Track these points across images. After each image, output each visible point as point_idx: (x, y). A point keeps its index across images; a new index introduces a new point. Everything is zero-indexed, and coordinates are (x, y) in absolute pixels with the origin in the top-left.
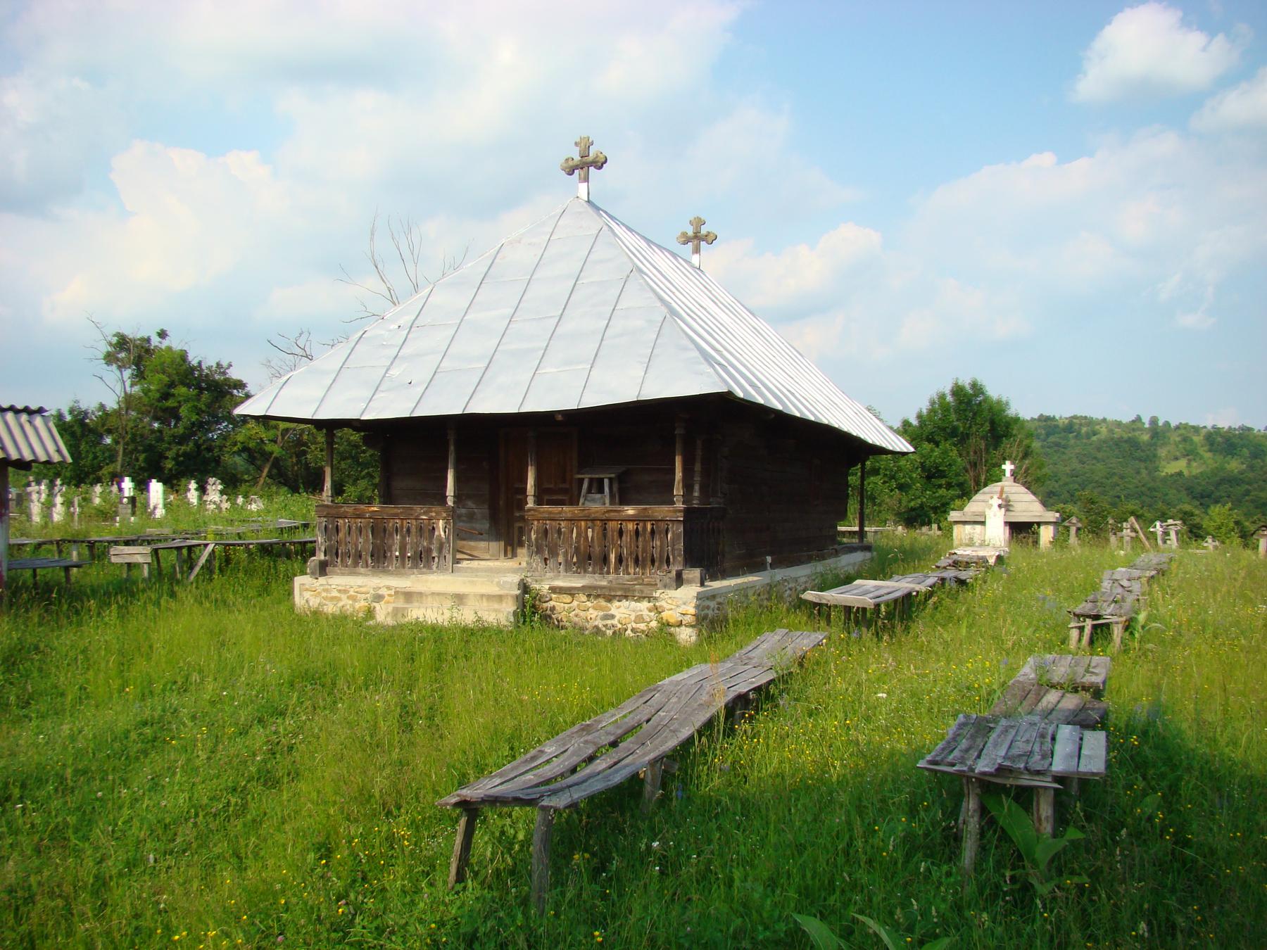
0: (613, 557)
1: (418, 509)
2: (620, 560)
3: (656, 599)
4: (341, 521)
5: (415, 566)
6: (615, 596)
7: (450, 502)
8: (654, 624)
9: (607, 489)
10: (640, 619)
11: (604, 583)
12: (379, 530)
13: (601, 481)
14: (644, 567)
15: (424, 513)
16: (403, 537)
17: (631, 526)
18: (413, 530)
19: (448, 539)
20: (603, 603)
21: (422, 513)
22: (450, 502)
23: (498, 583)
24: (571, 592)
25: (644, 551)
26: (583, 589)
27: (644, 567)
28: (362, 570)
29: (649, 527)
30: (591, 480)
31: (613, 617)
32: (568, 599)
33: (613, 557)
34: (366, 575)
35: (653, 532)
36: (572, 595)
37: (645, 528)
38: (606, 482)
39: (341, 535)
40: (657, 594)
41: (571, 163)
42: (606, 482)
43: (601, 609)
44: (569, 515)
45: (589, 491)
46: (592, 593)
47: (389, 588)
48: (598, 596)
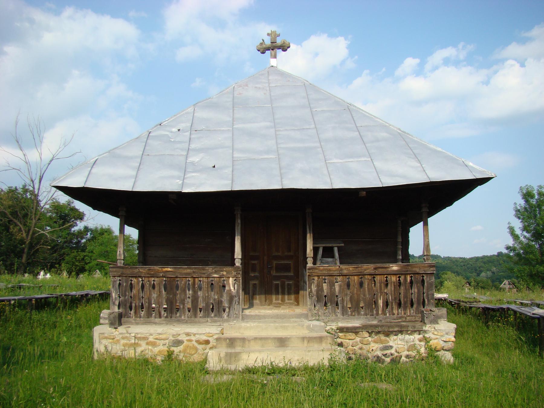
0: (381, 302)
1: (210, 269)
2: (386, 304)
3: (425, 332)
4: (134, 280)
5: (207, 316)
6: (392, 332)
7: (238, 263)
8: (423, 350)
9: (337, 255)
10: (412, 347)
11: (375, 322)
12: (171, 286)
13: (331, 249)
14: (405, 309)
15: (216, 272)
16: (195, 292)
17: (394, 279)
18: (204, 286)
19: (238, 292)
20: (383, 337)
21: (214, 273)
22: (238, 263)
23: (308, 327)
24: (355, 331)
25: (406, 296)
26: (364, 327)
27: (405, 309)
28: (158, 320)
29: (409, 279)
30: (324, 248)
31: (391, 347)
32: (352, 336)
33: (381, 302)
34: (160, 324)
35: (411, 282)
36: (356, 333)
37: (405, 279)
38: (336, 249)
39: (134, 291)
40: (427, 328)
41: (264, 46)
42: (336, 249)
43: (381, 342)
44: (345, 272)
45: (323, 256)
46: (372, 330)
47: (188, 334)
48: (379, 332)
